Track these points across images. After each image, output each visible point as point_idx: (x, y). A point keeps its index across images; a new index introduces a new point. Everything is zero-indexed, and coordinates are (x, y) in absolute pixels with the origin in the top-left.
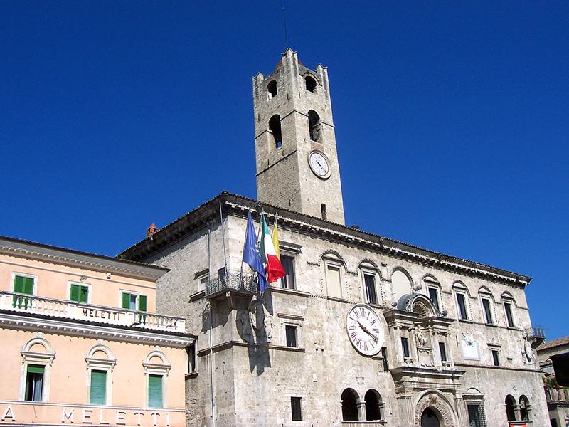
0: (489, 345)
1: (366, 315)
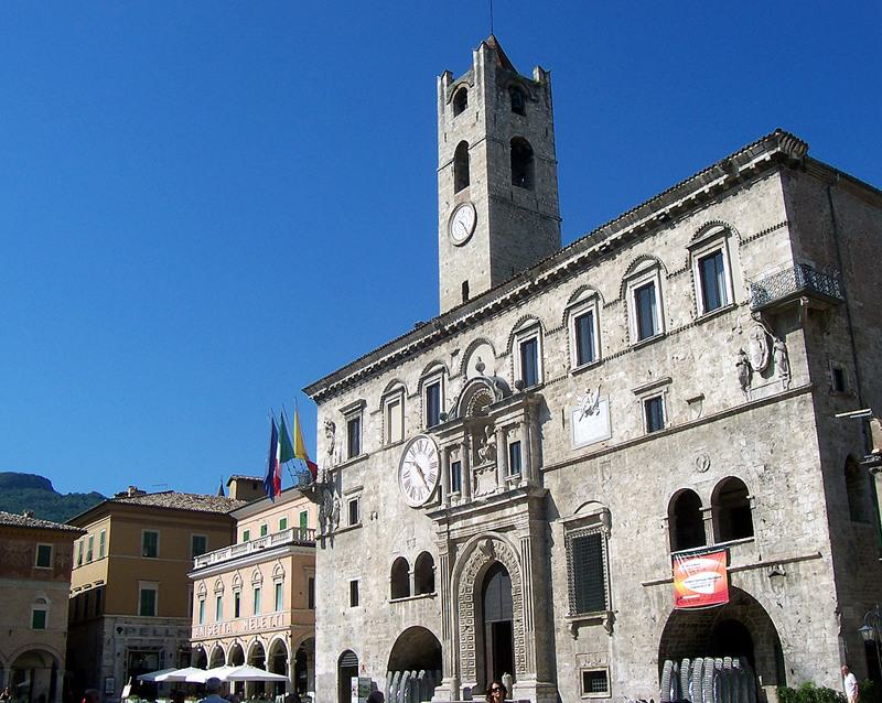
0: (637, 393)
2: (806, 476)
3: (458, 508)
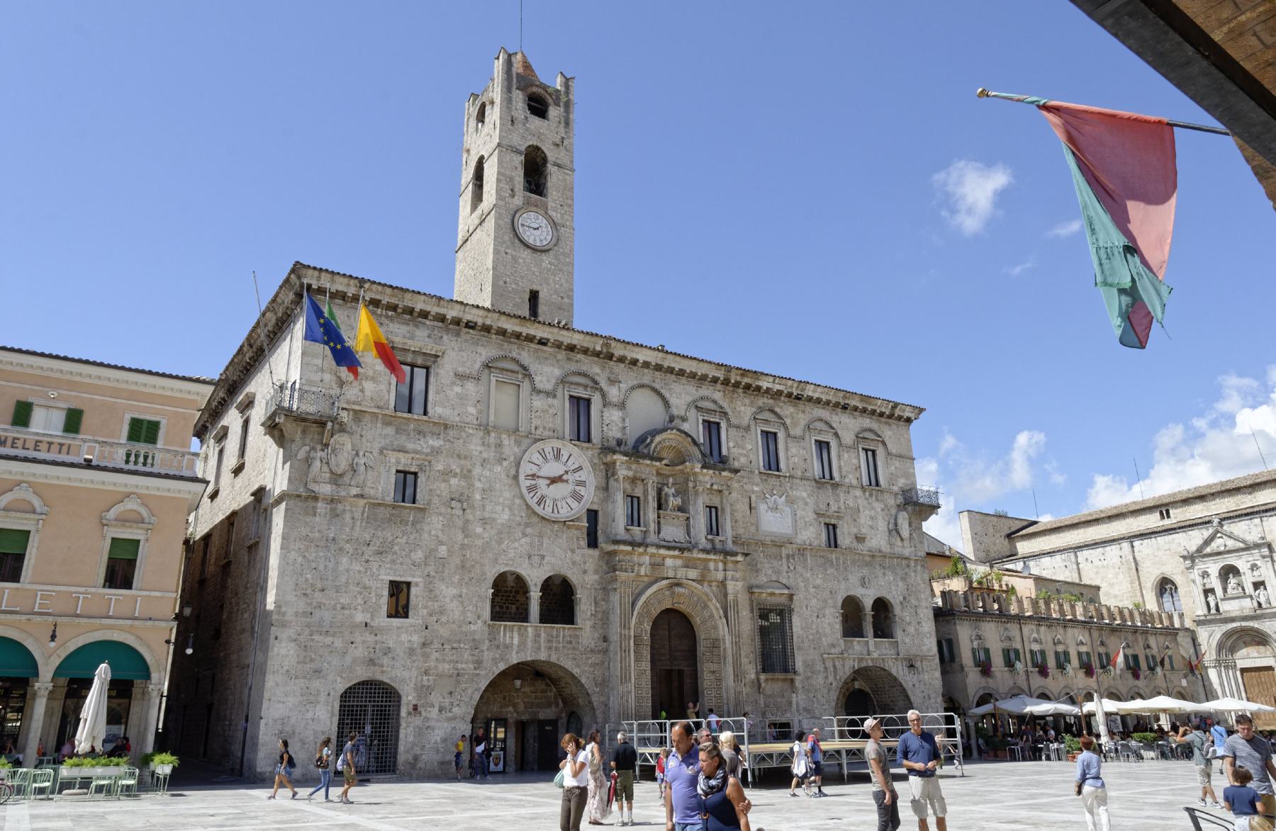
1: (564, 458)
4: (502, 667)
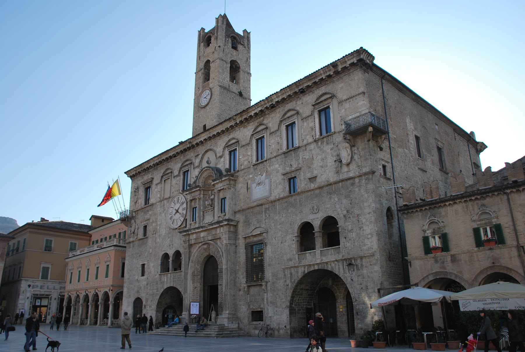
2: (368, 216)
3: (194, 229)
4: (162, 290)
